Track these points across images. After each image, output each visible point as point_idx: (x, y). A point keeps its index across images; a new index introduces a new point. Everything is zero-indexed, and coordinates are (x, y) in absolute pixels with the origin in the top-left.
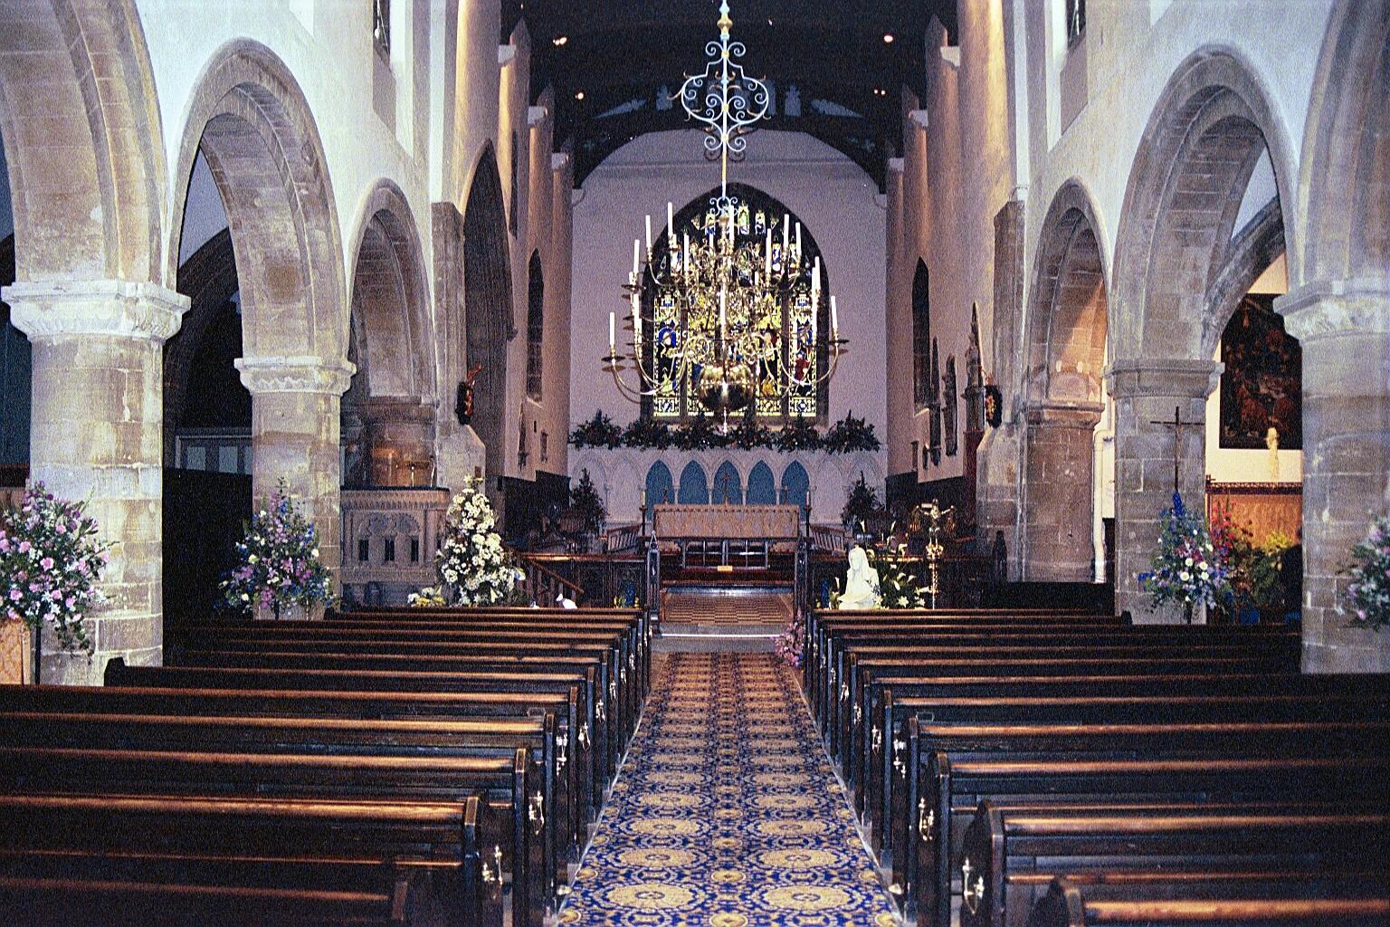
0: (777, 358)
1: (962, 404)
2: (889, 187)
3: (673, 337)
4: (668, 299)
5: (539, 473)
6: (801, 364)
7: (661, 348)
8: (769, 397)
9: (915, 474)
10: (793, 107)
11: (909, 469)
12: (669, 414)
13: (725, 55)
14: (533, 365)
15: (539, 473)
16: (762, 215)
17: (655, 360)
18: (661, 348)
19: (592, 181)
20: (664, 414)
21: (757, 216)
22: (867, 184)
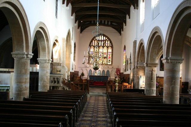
1: (129, 65)
5: (75, 71)
10: (110, 23)
13: (97, 28)
14: (74, 57)
15: (75, 71)
19: (83, 32)
22: (118, 34)
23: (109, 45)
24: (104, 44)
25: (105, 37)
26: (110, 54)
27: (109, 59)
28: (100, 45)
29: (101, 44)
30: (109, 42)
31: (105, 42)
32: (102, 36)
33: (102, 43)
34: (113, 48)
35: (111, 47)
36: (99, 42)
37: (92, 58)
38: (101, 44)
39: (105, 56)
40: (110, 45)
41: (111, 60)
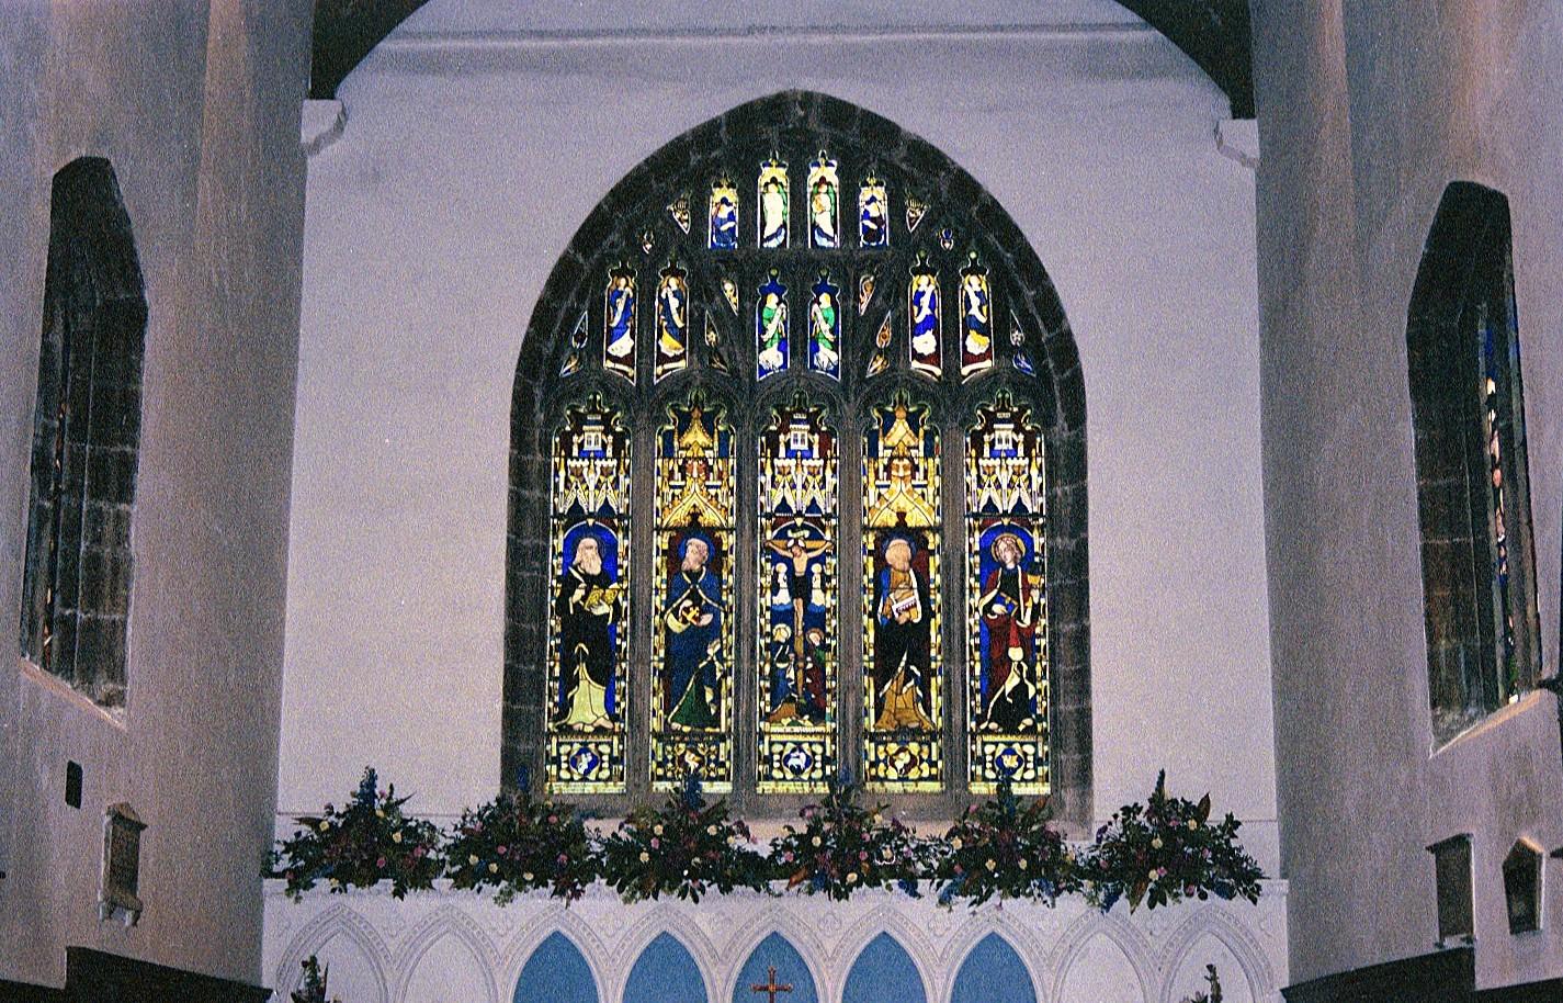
0: (928, 614)
2: (1265, 80)
3: (608, 552)
4: (593, 436)
6: (997, 634)
7: (569, 584)
8: (903, 734)
9: (1461, 963)
11: (1425, 939)
12: (589, 788)
15: (81, 958)
16: (880, 192)
17: (553, 623)
18: (569, 584)
19: (361, 84)
20: (577, 788)
21: (865, 194)
23: (976, 343)
24: (854, 335)
25: (874, 200)
26: (1006, 551)
27: (996, 668)
28: (771, 357)
29: (799, 339)
30: (973, 285)
31: (895, 292)
32: (825, 172)
33: (823, 311)
34: (1077, 419)
35: (1019, 384)
36: (752, 298)
37: (602, 675)
38: (799, 339)
39: (904, 604)
40: (1001, 348)
41: (1043, 705)
